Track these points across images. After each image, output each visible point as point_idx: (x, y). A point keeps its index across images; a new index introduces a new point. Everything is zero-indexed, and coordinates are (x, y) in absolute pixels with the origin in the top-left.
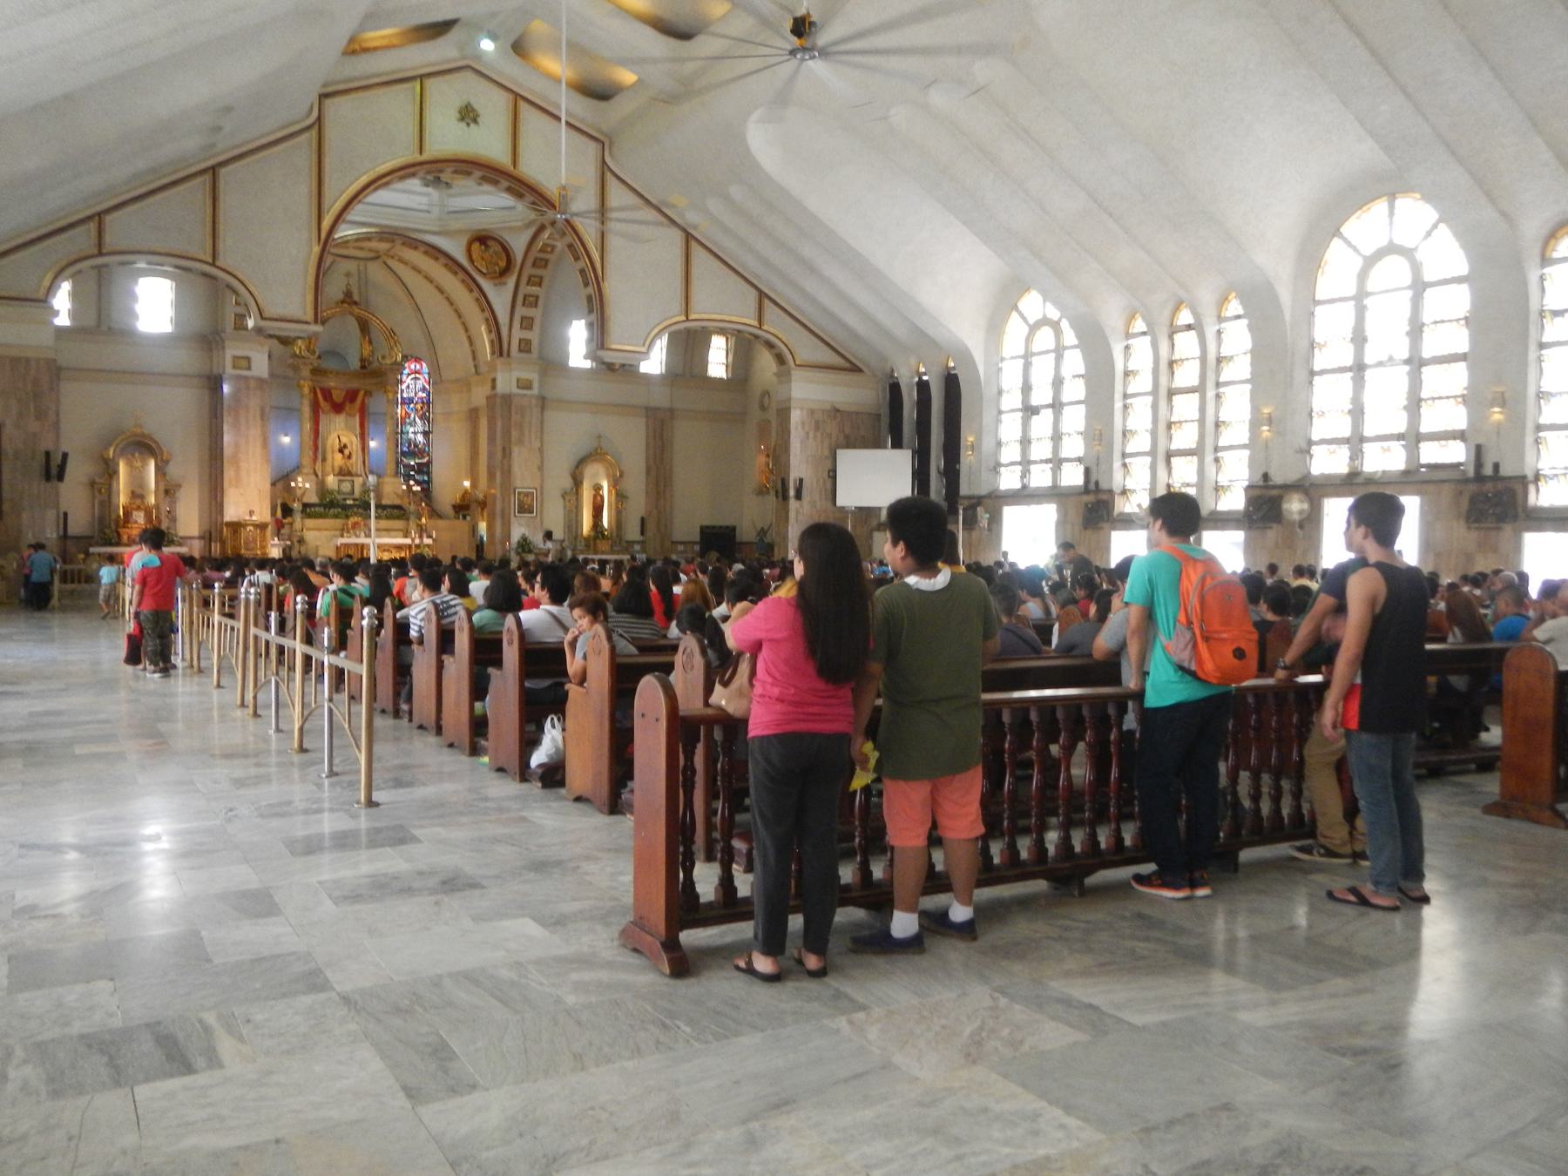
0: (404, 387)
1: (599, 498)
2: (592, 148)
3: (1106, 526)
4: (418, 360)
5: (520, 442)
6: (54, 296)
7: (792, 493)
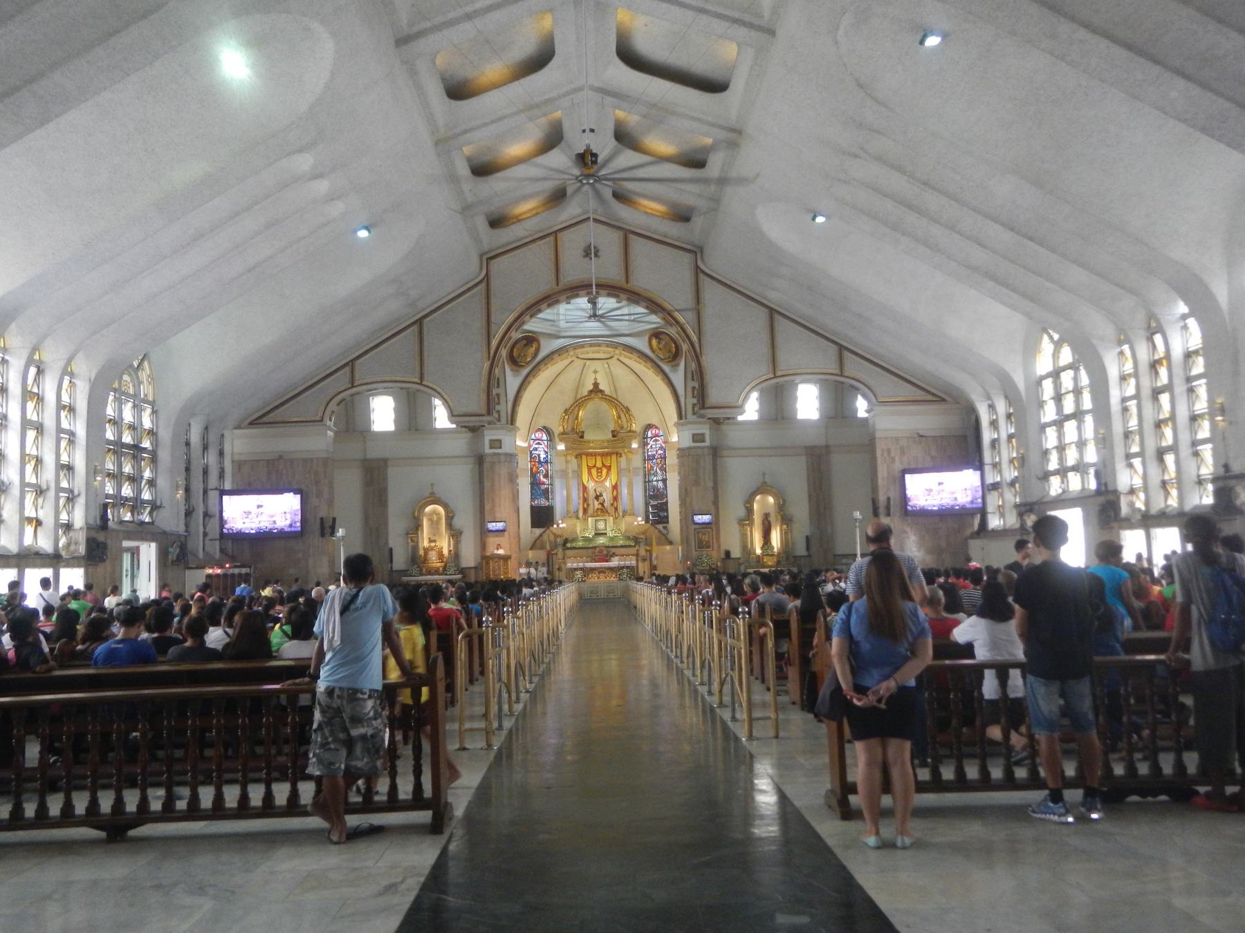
1: (766, 522)
2: (686, 258)
3: (1115, 525)
5: (697, 483)
6: (396, 410)
7: (882, 510)
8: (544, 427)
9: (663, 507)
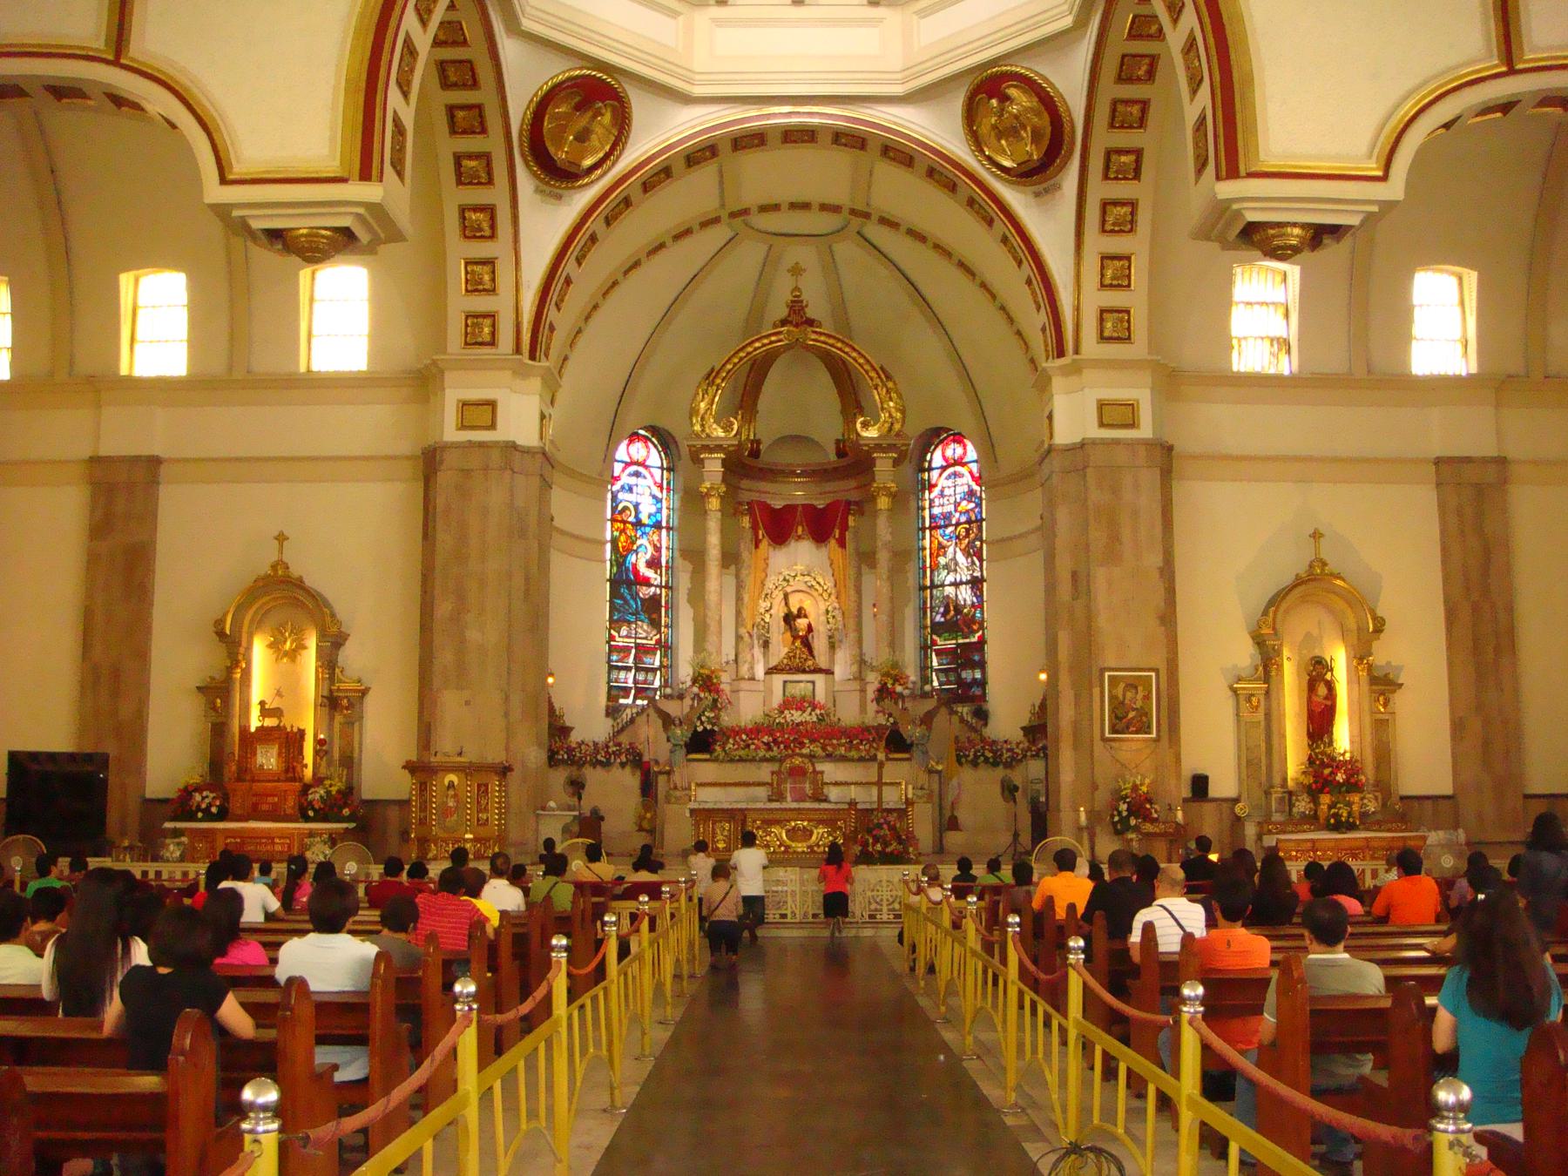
0: (936, 491)
4: (958, 438)
8: (654, 430)
9: (971, 656)
